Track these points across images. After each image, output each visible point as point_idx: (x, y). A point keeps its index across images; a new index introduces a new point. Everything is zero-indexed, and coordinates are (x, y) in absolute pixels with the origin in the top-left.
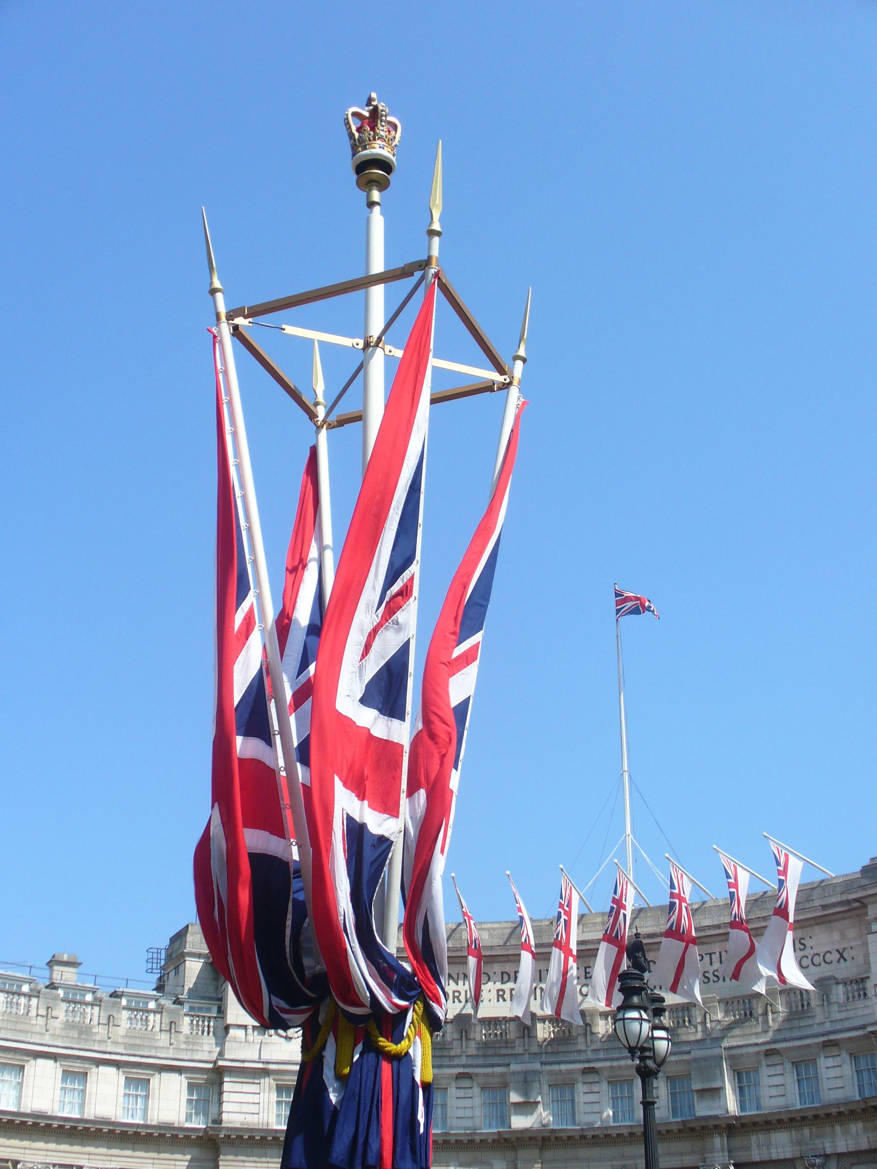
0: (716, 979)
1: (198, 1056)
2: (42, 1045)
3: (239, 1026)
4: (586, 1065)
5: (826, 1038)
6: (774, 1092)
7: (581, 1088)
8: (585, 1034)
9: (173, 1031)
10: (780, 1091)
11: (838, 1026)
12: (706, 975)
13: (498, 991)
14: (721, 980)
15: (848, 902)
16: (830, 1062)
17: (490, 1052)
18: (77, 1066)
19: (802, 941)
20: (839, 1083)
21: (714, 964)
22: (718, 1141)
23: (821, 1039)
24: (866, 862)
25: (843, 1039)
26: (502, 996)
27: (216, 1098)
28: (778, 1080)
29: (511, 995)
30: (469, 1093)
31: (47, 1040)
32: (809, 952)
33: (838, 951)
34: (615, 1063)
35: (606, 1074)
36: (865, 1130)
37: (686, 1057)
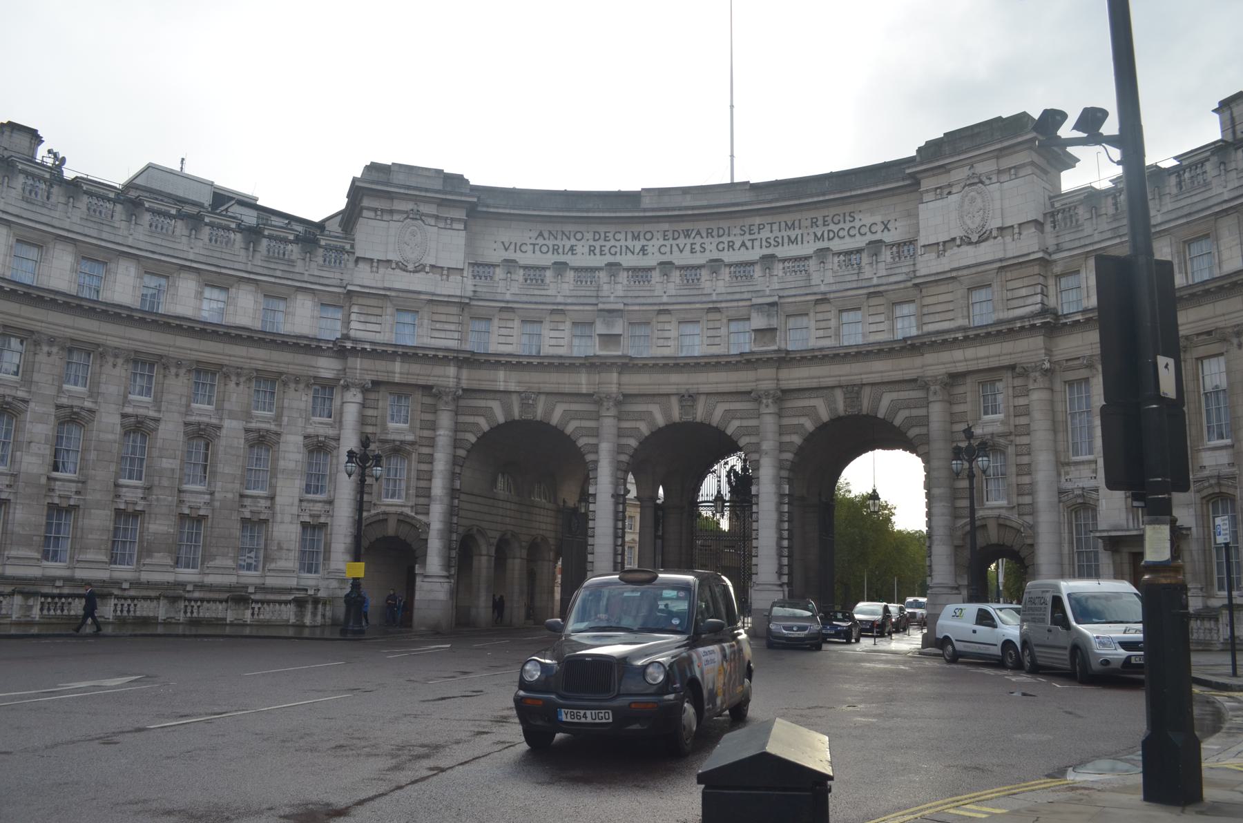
0: (776, 244)
2: (186, 259)
3: (364, 259)
9: (308, 259)
12: (768, 240)
13: (590, 246)
19: (852, 214)
21: (774, 232)
23: (865, 291)
24: (923, 144)
26: (593, 251)
29: (601, 251)
32: (857, 224)
33: (883, 222)
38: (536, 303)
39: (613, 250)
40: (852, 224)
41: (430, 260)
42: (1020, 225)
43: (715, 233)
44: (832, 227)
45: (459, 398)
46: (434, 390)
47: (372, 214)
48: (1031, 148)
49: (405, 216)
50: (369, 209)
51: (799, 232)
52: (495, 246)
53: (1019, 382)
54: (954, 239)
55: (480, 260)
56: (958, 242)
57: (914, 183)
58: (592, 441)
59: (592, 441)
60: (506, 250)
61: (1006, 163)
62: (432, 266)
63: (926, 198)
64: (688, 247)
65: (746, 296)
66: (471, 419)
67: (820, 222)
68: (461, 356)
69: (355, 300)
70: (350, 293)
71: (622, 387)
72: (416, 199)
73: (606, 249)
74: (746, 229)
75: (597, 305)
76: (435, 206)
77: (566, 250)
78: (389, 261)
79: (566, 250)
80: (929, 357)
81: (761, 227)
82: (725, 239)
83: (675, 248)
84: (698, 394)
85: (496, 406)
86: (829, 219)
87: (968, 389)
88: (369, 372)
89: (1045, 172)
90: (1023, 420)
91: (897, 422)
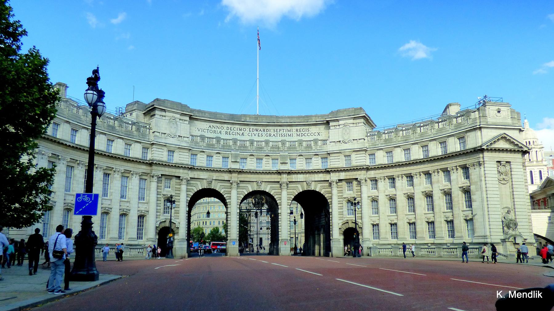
4: (251, 154)
5: (315, 153)
7: (248, 159)
10: (302, 165)
14: (286, 136)
15: (323, 121)
16: (316, 159)
17: (225, 147)
18: (112, 138)
20: (317, 164)
22: (285, 176)
34: (259, 154)
35: (256, 156)
36: (323, 176)
37: (279, 154)
39: (233, 133)
40: (308, 132)
42: (359, 139)
43: (265, 131)
44: (302, 132)
45: (188, 180)
47: (158, 117)
48: (363, 118)
51: (292, 133)
52: (195, 129)
54: (340, 141)
55: (192, 134)
56: (341, 142)
57: (328, 123)
58: (229, 195)
59: (229, 195)
61: (355, 121)
62: (179, 136)
63: (331, 128)
64: (257, 134)
66: (190, 188)
67: (299, 131)
68: (190, 167)
69: (154, 146)
70: (153, 144)
71: (239, 178)
73: (231, 133)
74: (276, 130)
75: (231, 152)
77: (218, 132)
78: (165, 133)
79: (218, 132)
81: (280, 130)
82: (269, 133)
83: (253, 134)
85: (198, 183)
86: (301, 130)
87: (344, 183)
88: (160, 171)
89: (365, 125)
90: (360, 193)
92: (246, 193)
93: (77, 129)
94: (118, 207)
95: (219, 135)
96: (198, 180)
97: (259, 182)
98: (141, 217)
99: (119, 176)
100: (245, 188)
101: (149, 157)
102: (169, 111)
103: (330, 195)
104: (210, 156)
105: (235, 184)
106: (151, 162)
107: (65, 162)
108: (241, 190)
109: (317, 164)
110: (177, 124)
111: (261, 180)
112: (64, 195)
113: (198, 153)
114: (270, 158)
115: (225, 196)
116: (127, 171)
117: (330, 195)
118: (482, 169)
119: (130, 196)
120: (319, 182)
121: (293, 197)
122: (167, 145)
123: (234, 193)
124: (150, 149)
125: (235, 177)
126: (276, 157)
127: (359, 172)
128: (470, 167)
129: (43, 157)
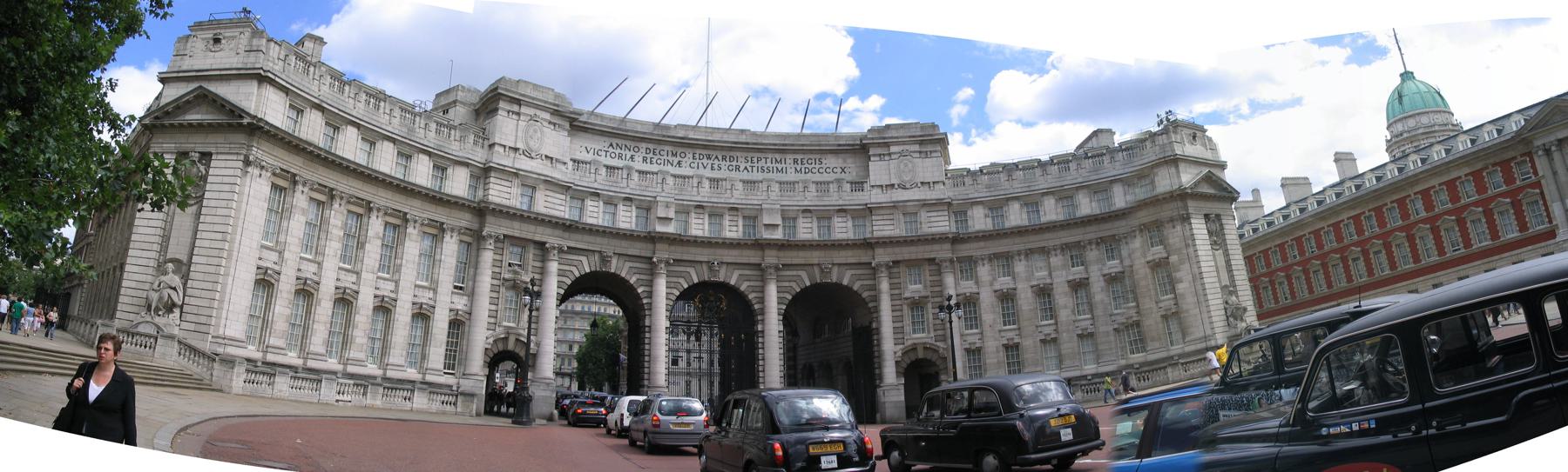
1: (476, 159)
3: (501, 145)
6: (805, 230)
7: (693, 215)
8: (698, 187)
10: (810, 230)
11: (847, 203)
16: (840, 219)
20: (844, 230)
25: (850, 209)
27: (482, 186)
28: (809, 225)
30: (629, 209)
31: (390, 129)
34: (715, 205)
35: (708, 210)
38: (615, 192)
41: (545, 152)
46: (547, 245)
47: (505, 114)
49: (529, 118)
50: (503, 109)
53: (934, 267)
59: (647, 289)
60: (588, 152)
62: (546, 156)
65: (756, 202)
68: (568, 223)
72: (537, 107)
76: (549, 114)
78: (516, 149)
79: (628, 158)
80: (879, 251)
84: (722, 263)
85: (584, 259)
87: (902, 269)
91: (855, 288)
92: (686, 286)
93: (337, 123)
94: (410, 298)
95: (631, 164)
96: (582, 252)
97: (716, 263)
98: (458, 325)
99: (415, 232)
100: (683, 274)
101: (480, 193)
102: (529, 105)
103: (872, 293)
104: (610, 202)
105: (663, 265)
106: (484, 205)
107: (306, 190)
108: (675, 280)
109: (844, 230)
110: (542, 132)
111: (720, 259)
112: (298, 259)
113: (587, 198)
114: (739, 213)
115: (640, 290)
116: (433, 223)
117: (872, 293)
118: (1188, 227)
119: (435, 276)
120: (846, 267)
121: (790, 297)
122: (521, 173)
123: (661, 286)
124: (482, 181)
125: (662, 253)
126: (753, 213)
127: (936, 247)
128: (1166, 225)
129: (264, 172)
